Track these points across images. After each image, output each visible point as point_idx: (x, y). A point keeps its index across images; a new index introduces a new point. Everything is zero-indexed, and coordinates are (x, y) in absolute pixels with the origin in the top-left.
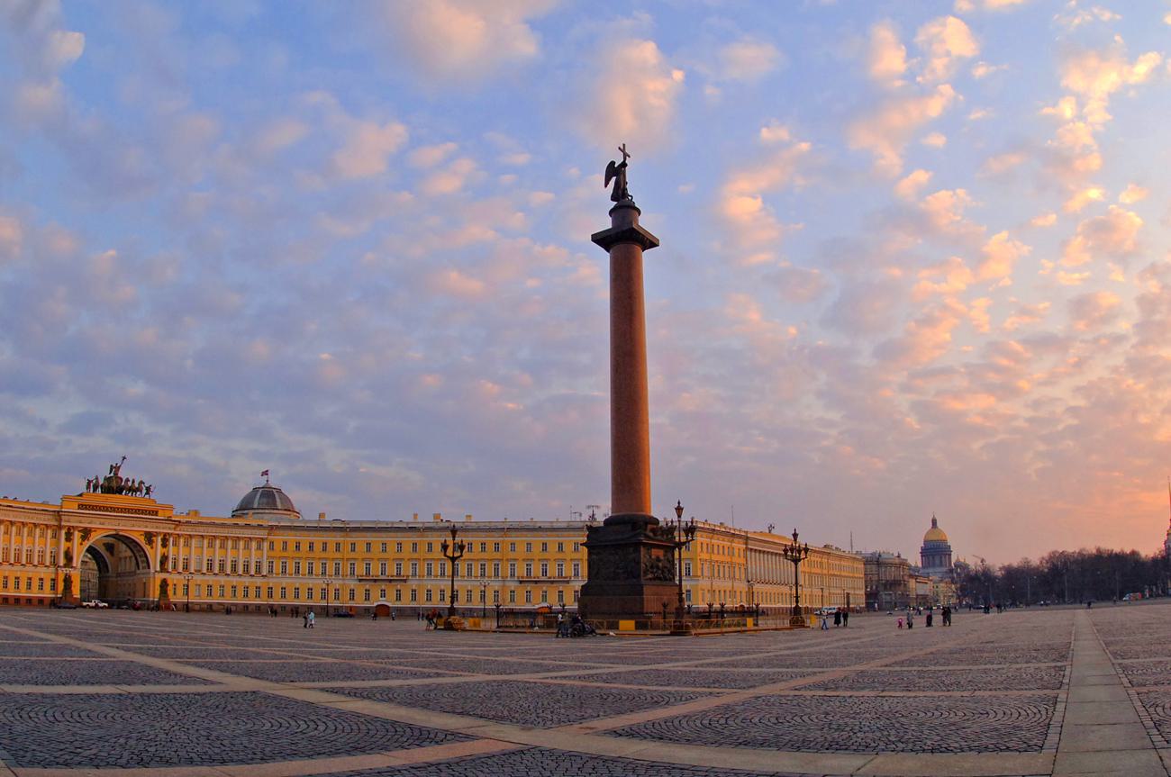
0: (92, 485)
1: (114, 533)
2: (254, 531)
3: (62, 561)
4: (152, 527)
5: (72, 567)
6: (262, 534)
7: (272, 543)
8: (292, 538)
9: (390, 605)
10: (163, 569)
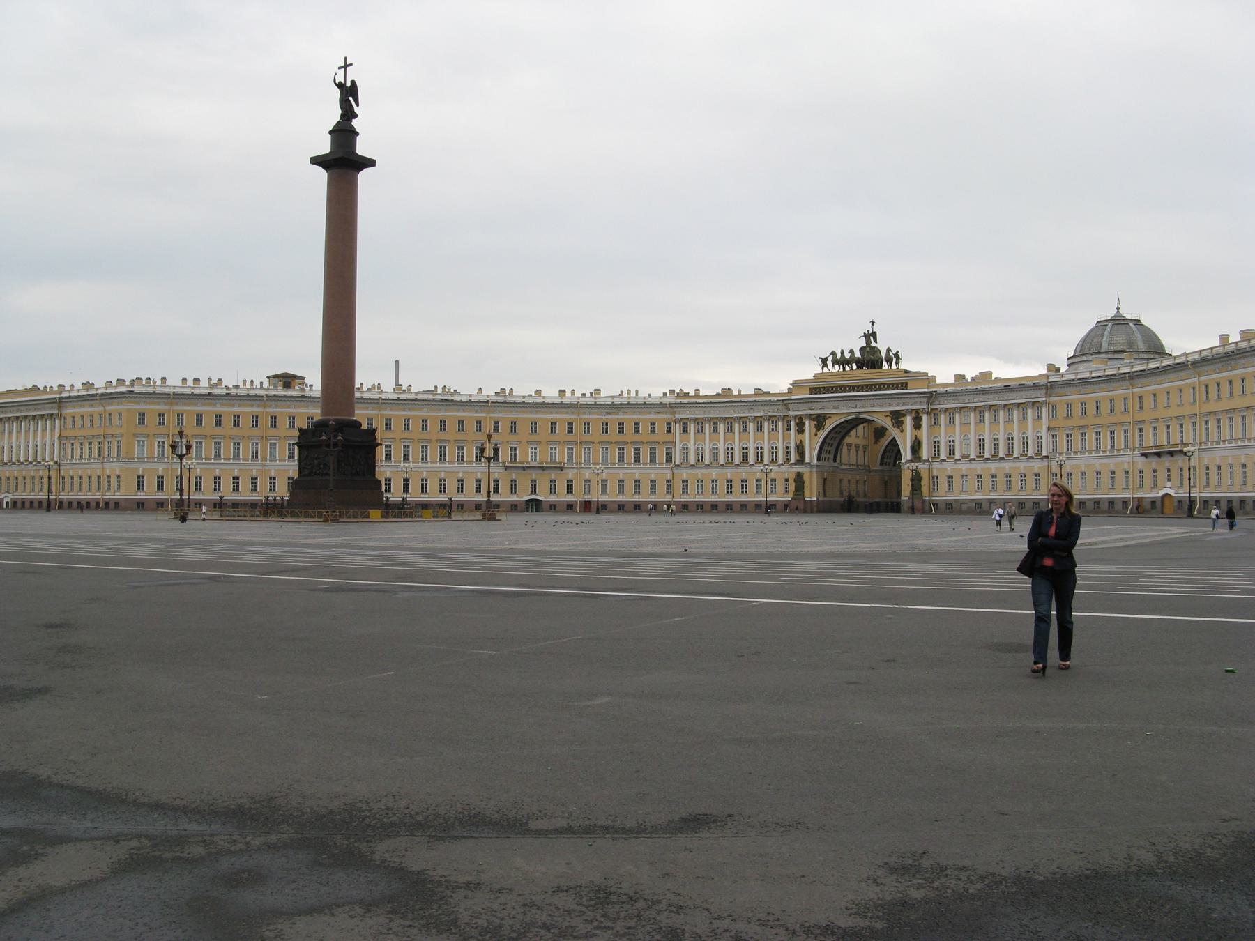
2: (1029, 393)
6: (1038, 396)
8: (1075, 397)
9: (1172, 492)
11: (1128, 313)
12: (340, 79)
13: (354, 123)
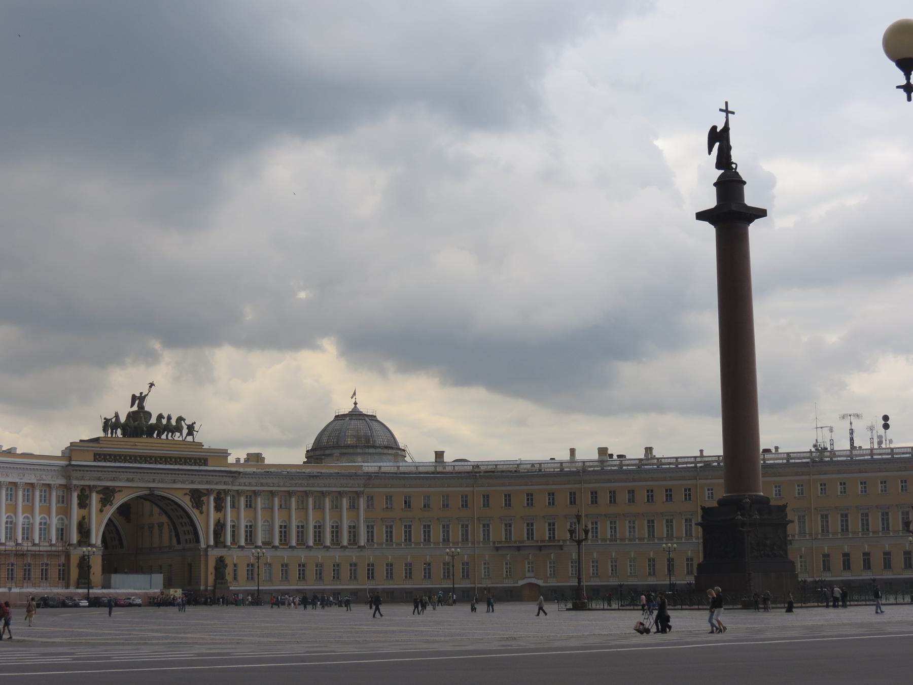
0: (109, 425)
3: (75, 538)
4: (200, 483)
5: (90, 545)
7: (370, 499)
9: (540, 583)
10: (219, 541)
11: (364, 408)
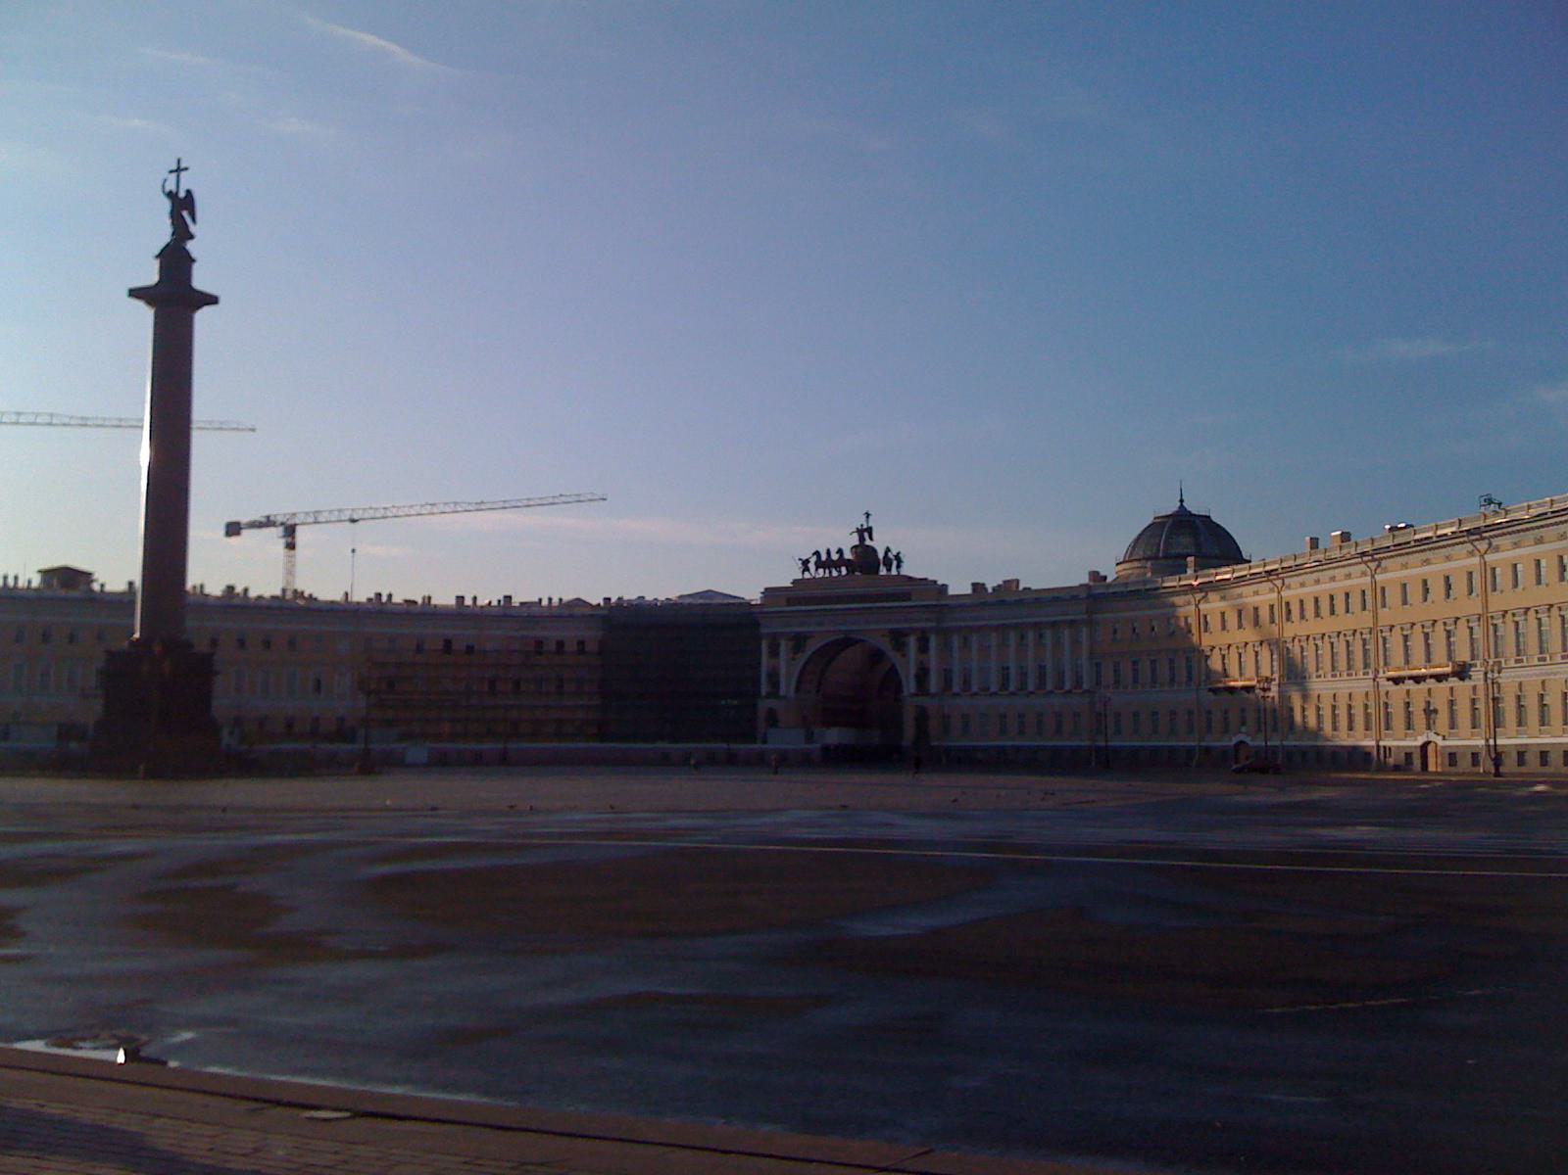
1: (842, 636)
9: (1248, 740)
11: (1194, 507)
12: (171, 186)
13: (190, 246)
